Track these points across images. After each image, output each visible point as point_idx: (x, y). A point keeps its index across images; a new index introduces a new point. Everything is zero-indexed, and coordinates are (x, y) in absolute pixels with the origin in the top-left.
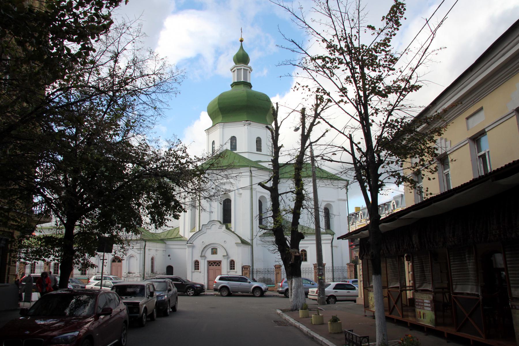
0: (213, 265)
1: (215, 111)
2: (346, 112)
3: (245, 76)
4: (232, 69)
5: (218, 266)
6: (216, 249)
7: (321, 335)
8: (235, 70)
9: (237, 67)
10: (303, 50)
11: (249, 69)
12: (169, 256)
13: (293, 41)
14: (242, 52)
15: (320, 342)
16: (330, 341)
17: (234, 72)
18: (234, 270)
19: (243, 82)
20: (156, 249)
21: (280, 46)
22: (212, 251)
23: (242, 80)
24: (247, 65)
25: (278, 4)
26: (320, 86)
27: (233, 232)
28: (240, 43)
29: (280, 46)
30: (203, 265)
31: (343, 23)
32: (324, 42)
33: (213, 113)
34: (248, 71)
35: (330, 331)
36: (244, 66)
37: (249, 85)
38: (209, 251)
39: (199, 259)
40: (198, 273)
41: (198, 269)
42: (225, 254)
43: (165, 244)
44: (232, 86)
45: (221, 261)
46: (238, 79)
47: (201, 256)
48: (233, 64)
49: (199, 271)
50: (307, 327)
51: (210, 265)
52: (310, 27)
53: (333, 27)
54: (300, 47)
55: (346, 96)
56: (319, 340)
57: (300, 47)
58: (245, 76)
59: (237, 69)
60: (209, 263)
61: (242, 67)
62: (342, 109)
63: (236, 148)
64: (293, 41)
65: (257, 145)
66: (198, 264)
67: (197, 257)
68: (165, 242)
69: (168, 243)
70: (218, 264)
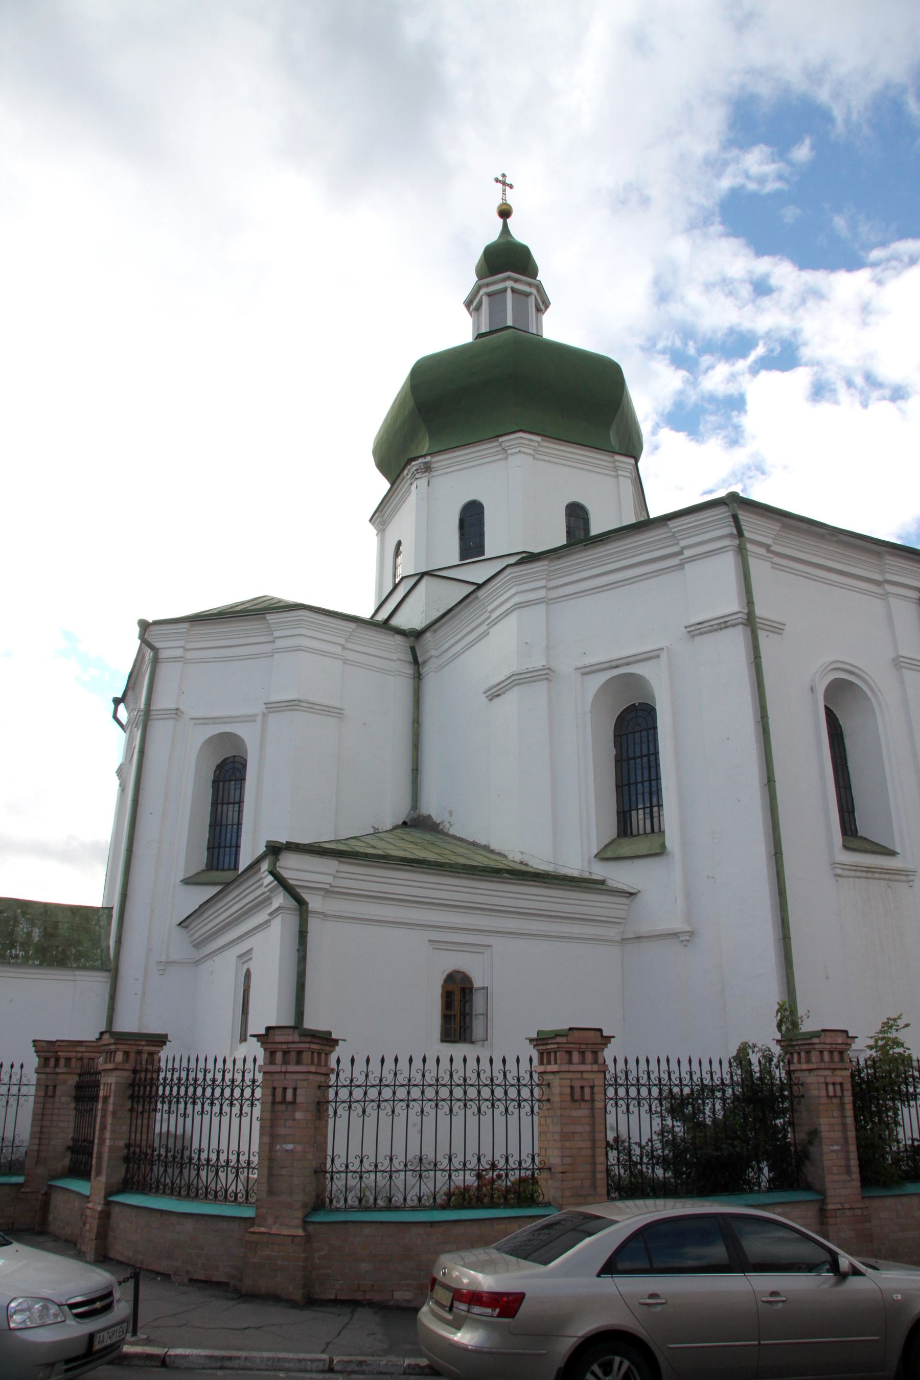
3: (522, 312)
9: (488, 285)
11: (534, 291)
34: (532, 300)
36: (516, 281)
59: (489, 295)
61: (509, 284)
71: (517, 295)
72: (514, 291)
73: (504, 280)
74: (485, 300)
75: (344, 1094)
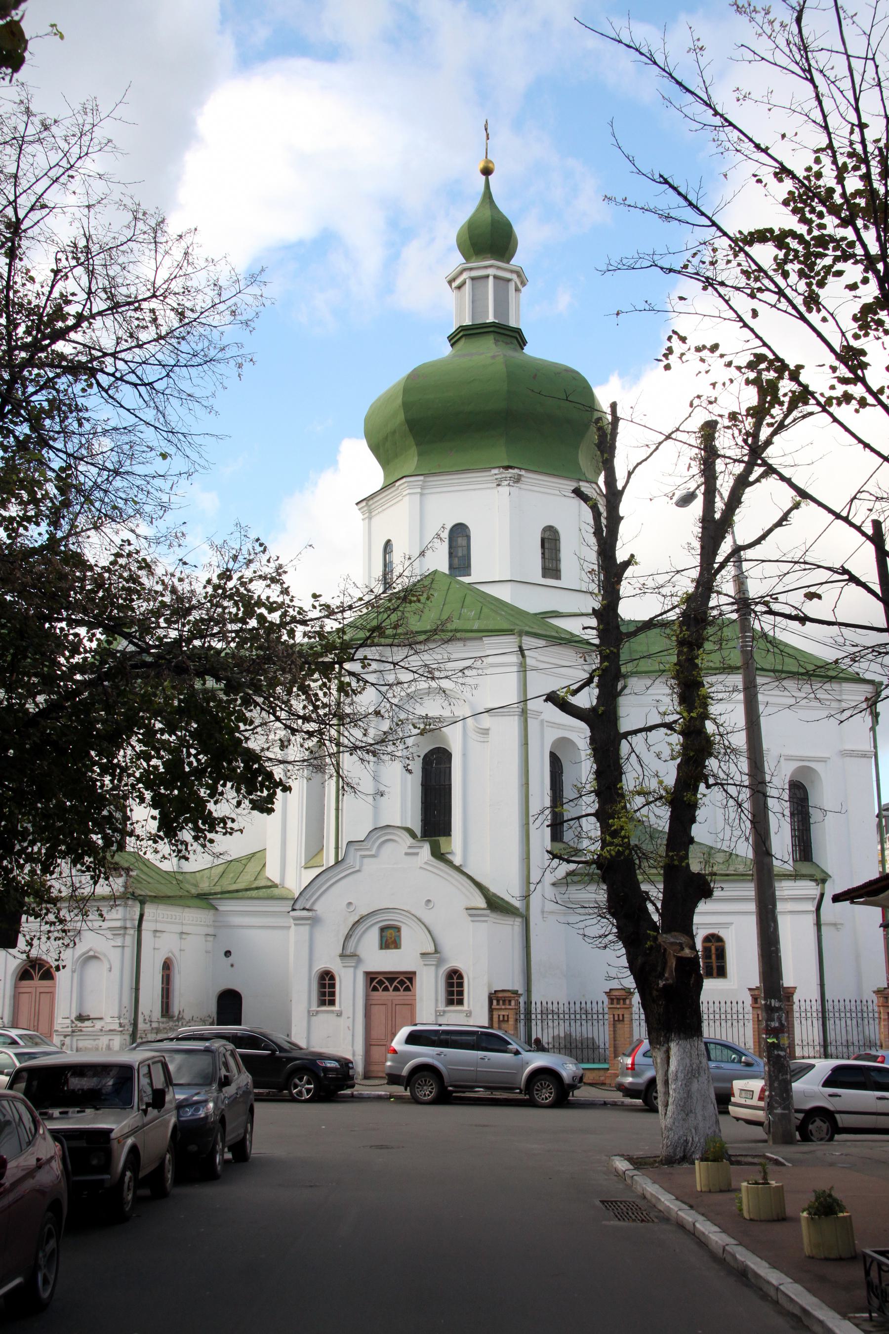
0: (386, 989)
1: (394, 433)
2: (860, 441)
3: (502, 303)
4: (454, 280)
5: (402, 992)
6: (398, 929)
7: (774, 1265)
8: (464, 283)
9: (471, 269)
10: (703, 214)
11: (514, 277)
12: (228, 953)
13: (666, 182)
14: (487, 213)
15: (772, 1293)
16: (809, 1290)
17: (459, 287)
18: (459, 1008)
19: (493, 325)
20: (179, 929)
21: (619, 200)
22: (381, 937)
24: (508, 262)
25: (614, 35)
26: (765, 345)
27: (458, 869)
28: (484, 178)
29: (619, 200)
31: (857, 100)
32: (780, 180)
33: (386, 439)
34: (512, 286)
35: (807, 1250)
36: (499, 268)
37: (516, 337)
38: (373, 936)
40: (332, 1017)
41: (332, 1003)
42: (430, 948)
43: (212, 912)
44: (453, 340)
45: (414, 973)
46: (474, 315)
47: (342, 956)
48: (458, 259)
49: (337, 1008)
50: (724, 1231)
51: (375, 989)
52: (731, 124)
53: (820, 119)
54: (691, 204)
55: (863, 381)
56: (769, 1283)
57: (691, 204)
58: (502, 303)
59: (473, 279)
60: (372, 980)
61: (491, 272)
62: (847, 430)
63: (468, 566)
64: (666, 182)
65: (543, 554)
66: (333, 986)
67: (328, 960)
68: (214, 902)
69: (226, 906)
70: (402, 983)
71: (497, 281)
72: (495, 277)
73: (486, 267)
74: (468, 283)
75: (606, 1017)
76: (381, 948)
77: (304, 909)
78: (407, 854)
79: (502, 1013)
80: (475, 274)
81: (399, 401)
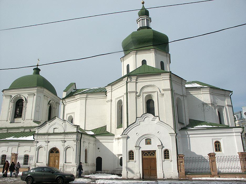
0: (148, 155)
5: (152, 156)
6: (151, 140)
18: (168, 159)
22: (146, 142)
23: (146, 26)
30: (138, 156)
34: (149, 21)
39: (133, 149)
45: (156, 151)
51: (144, 155)
59: (142, 19)
60: (144, 153)
67: (131, 147)
70: (152, 153)
72: (146, 19)
76: (146, 144)
77: (125, 135)
78: (152, 120)
79: (181, 160)
80: (142, 18)
81: (131, 37)
